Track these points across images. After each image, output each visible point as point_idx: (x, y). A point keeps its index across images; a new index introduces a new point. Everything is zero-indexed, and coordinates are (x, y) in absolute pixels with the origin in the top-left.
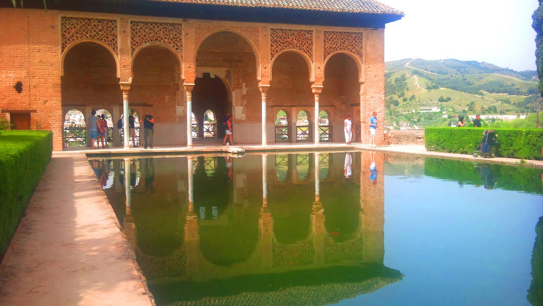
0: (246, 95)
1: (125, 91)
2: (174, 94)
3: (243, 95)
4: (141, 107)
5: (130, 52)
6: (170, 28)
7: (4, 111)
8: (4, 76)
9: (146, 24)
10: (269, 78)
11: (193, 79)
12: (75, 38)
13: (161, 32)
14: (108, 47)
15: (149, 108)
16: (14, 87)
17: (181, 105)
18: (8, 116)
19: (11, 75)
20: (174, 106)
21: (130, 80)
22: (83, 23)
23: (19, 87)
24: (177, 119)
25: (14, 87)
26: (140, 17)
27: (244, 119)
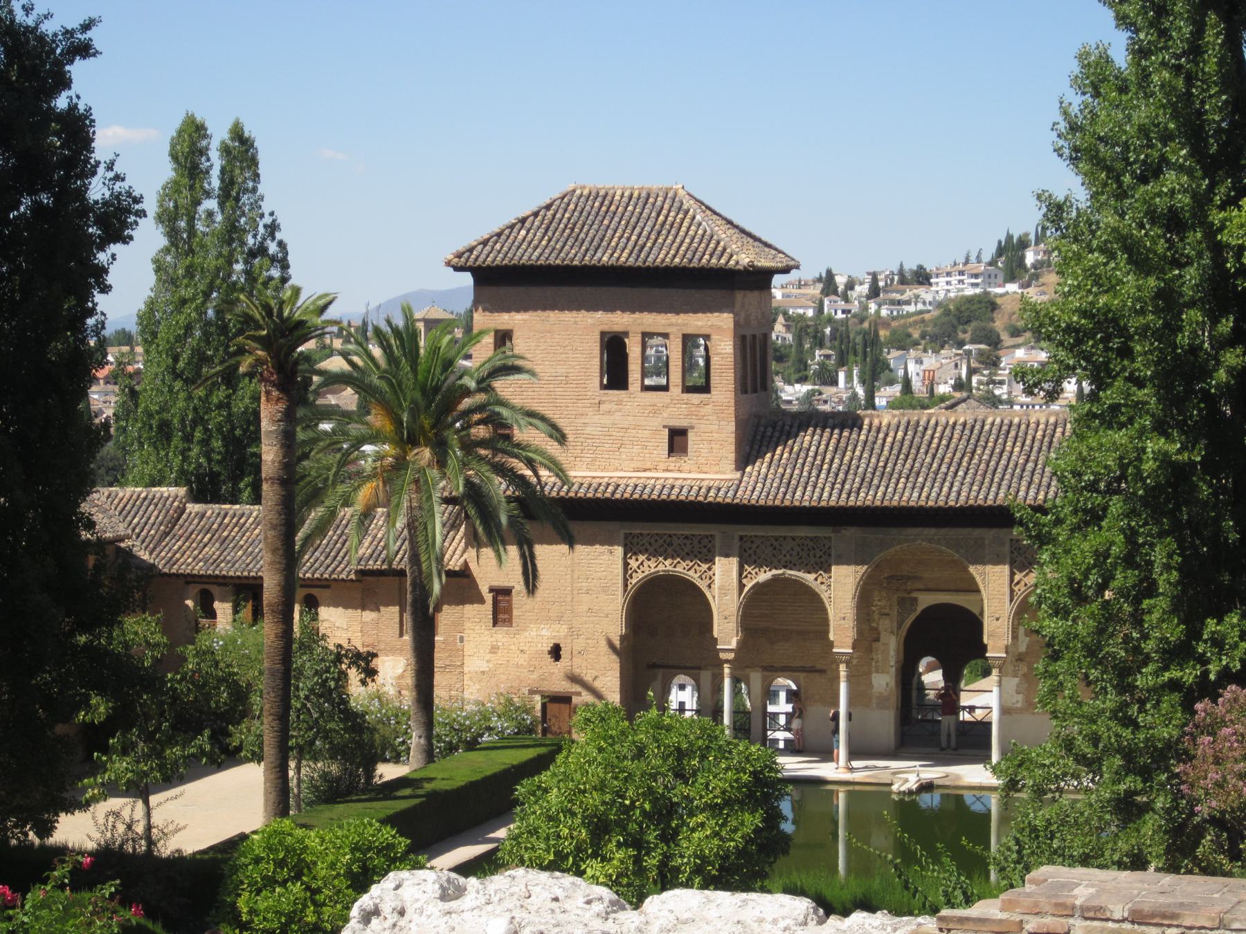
0: (1027, 653)
1: (727, 661)
2: (870, 650)
3: (1020, 654)
4: (802, 675)
5: (736, 592)
6: (811, 544)
7: (532, 692)
8: (534, 634)
9: (767, 538)
10: (1007, 640)
11: (850, 641)
12: (645, 568)
13: (794, 553)
14: (699, 583)
15: (817, 675)
16: (550, 652)
17: (883, 672)
18: (538, 698)
19: (544, 632)
20: (869, 673)
21: (733, 645)
22: (660, 542)
23: (556, 652)
24: (874, 701)
25: (550, 652)
26: (755, 527)
27: (1019, 705)
